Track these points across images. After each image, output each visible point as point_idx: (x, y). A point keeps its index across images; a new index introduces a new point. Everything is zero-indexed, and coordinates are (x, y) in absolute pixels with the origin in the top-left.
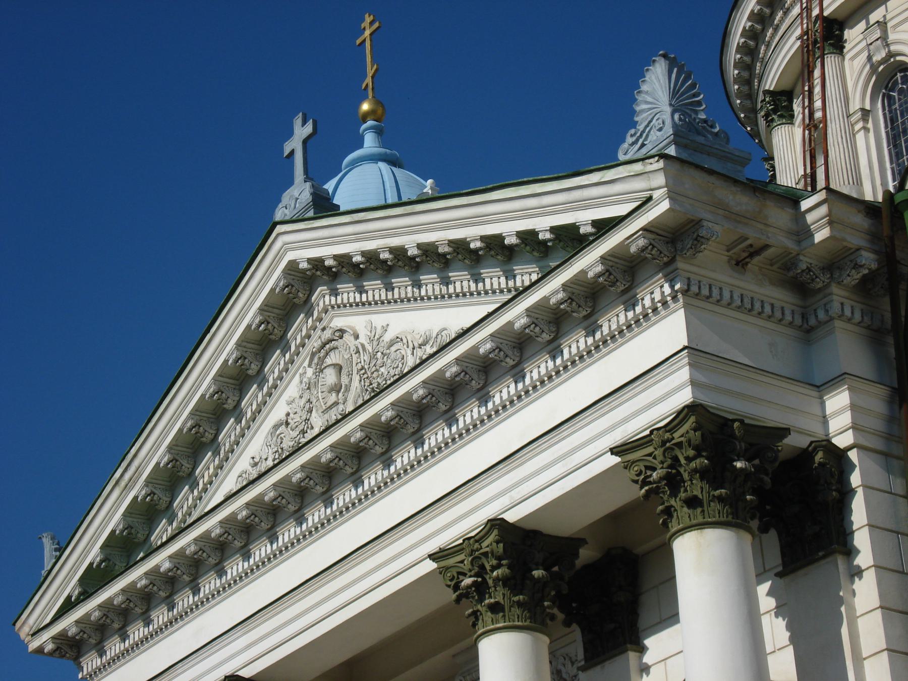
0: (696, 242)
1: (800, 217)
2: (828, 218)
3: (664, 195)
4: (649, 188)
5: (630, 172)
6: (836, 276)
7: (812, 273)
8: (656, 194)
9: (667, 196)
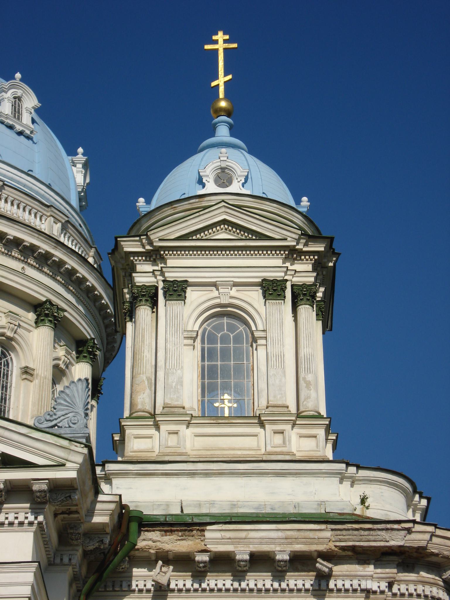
0: (65, 499)
1: (95, 501)
2: (111, 512)
3: (76, 468)
4: (66, 459)
5: (55, 442)
6: (86, 542)
7: (79, 536)
8: (69, 465)
9: (77, 470)
